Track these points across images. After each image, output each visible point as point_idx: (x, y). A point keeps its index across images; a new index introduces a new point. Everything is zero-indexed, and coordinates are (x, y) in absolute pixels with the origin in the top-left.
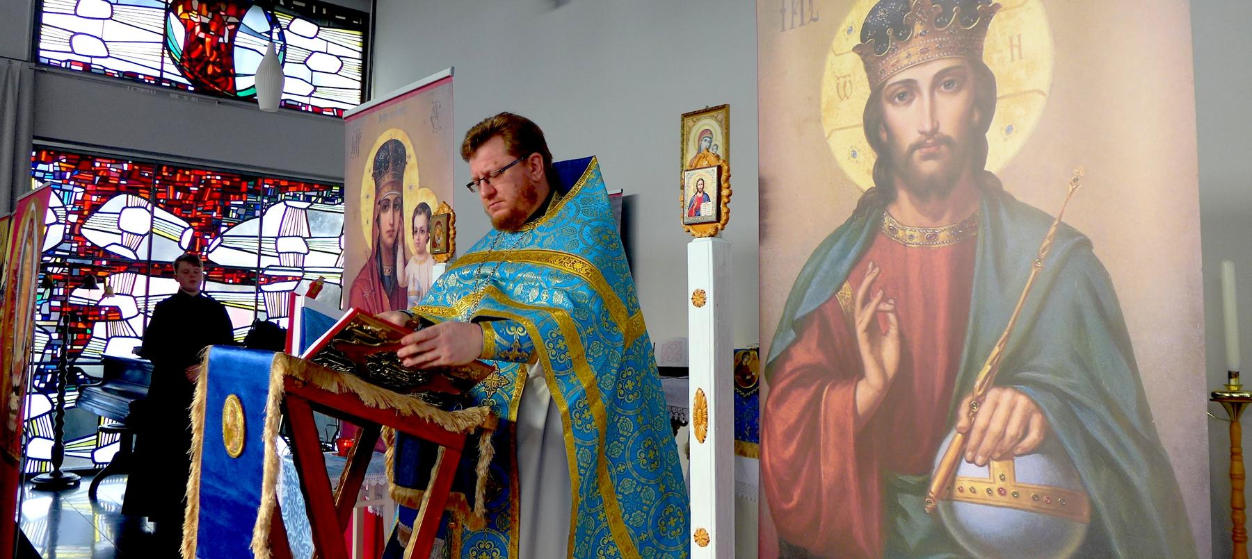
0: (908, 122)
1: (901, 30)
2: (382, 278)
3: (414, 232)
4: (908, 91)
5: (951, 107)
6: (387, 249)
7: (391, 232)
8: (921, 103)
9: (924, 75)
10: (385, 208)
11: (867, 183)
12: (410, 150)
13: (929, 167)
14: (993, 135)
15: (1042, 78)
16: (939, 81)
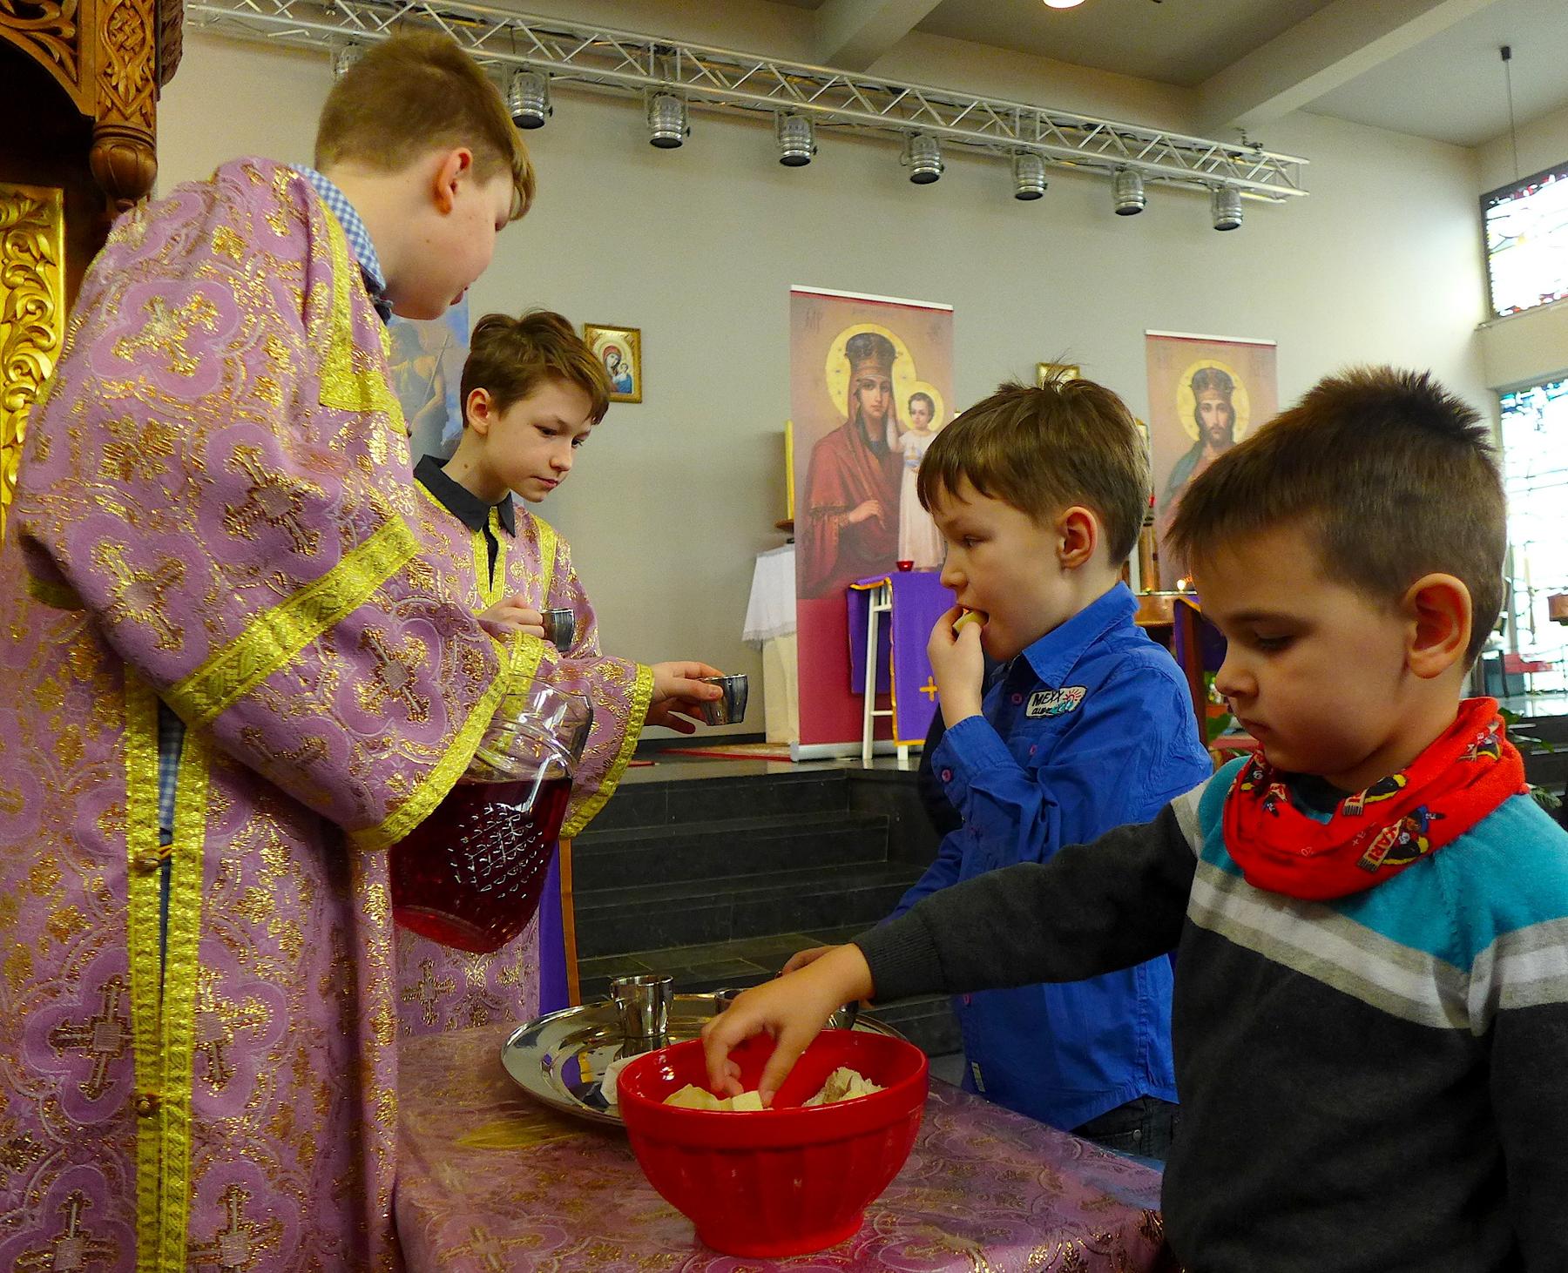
0: (1210, 418)
1: (1206, 386)
2: (866, 441)
3: (912, 412)
4: (1208, 408)
5: (1222, 417)
6: (873, 419)
7: (878, 407)
8: (1214, 411)
9: (1214, 403)
10: (869, 385)
11: (1196, 438)
12: (899, 347)
13: (1217, 436)
14: (1235, 430)
15: (1246, 415)
16: (1219, 407)
